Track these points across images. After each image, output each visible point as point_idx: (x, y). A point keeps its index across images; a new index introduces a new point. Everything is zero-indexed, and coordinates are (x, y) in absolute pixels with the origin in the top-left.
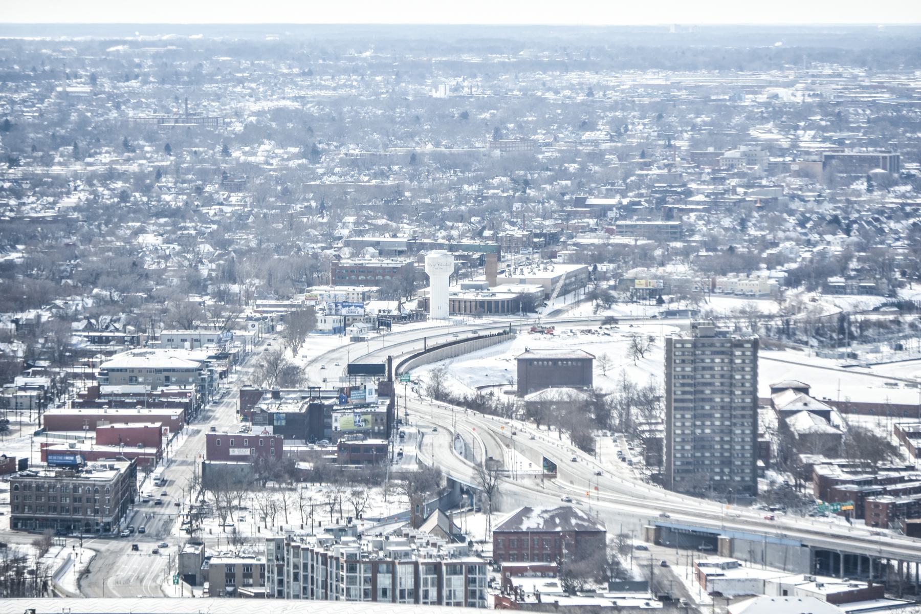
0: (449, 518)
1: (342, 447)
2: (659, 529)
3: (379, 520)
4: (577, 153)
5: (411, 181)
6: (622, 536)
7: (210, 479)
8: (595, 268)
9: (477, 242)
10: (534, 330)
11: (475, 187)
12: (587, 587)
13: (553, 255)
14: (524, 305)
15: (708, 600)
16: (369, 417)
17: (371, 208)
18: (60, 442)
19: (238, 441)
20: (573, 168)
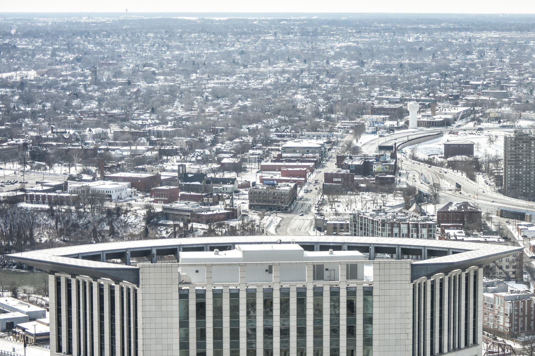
0: (420, 206)
1: (377, 178)
2: (502, 211)
3: (392, 207)
4: (465, 64)
5: (401, 74)
6: (488, 214)
7: (326, 190)
8: (474, 109)
9: (427, 98)
10: (450, 133)
11: (426, 77)
12: (474, 233)
13: (457, 104)
14: (446, 123)
15: (521, 238)
16: (387, 166)
17: (385, 85)
18: (267, 175)
19: (337, 175)
20: (464, 69)
